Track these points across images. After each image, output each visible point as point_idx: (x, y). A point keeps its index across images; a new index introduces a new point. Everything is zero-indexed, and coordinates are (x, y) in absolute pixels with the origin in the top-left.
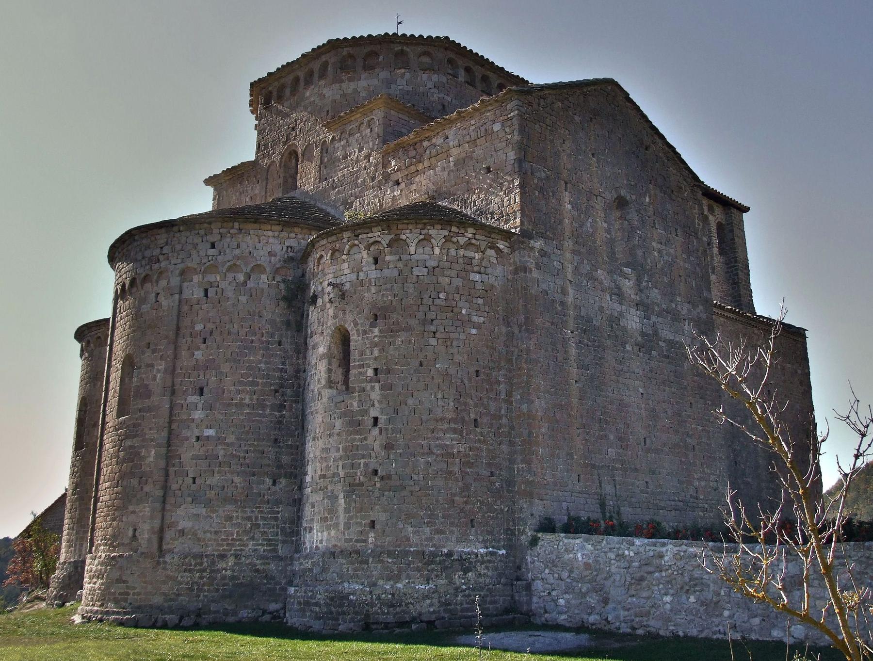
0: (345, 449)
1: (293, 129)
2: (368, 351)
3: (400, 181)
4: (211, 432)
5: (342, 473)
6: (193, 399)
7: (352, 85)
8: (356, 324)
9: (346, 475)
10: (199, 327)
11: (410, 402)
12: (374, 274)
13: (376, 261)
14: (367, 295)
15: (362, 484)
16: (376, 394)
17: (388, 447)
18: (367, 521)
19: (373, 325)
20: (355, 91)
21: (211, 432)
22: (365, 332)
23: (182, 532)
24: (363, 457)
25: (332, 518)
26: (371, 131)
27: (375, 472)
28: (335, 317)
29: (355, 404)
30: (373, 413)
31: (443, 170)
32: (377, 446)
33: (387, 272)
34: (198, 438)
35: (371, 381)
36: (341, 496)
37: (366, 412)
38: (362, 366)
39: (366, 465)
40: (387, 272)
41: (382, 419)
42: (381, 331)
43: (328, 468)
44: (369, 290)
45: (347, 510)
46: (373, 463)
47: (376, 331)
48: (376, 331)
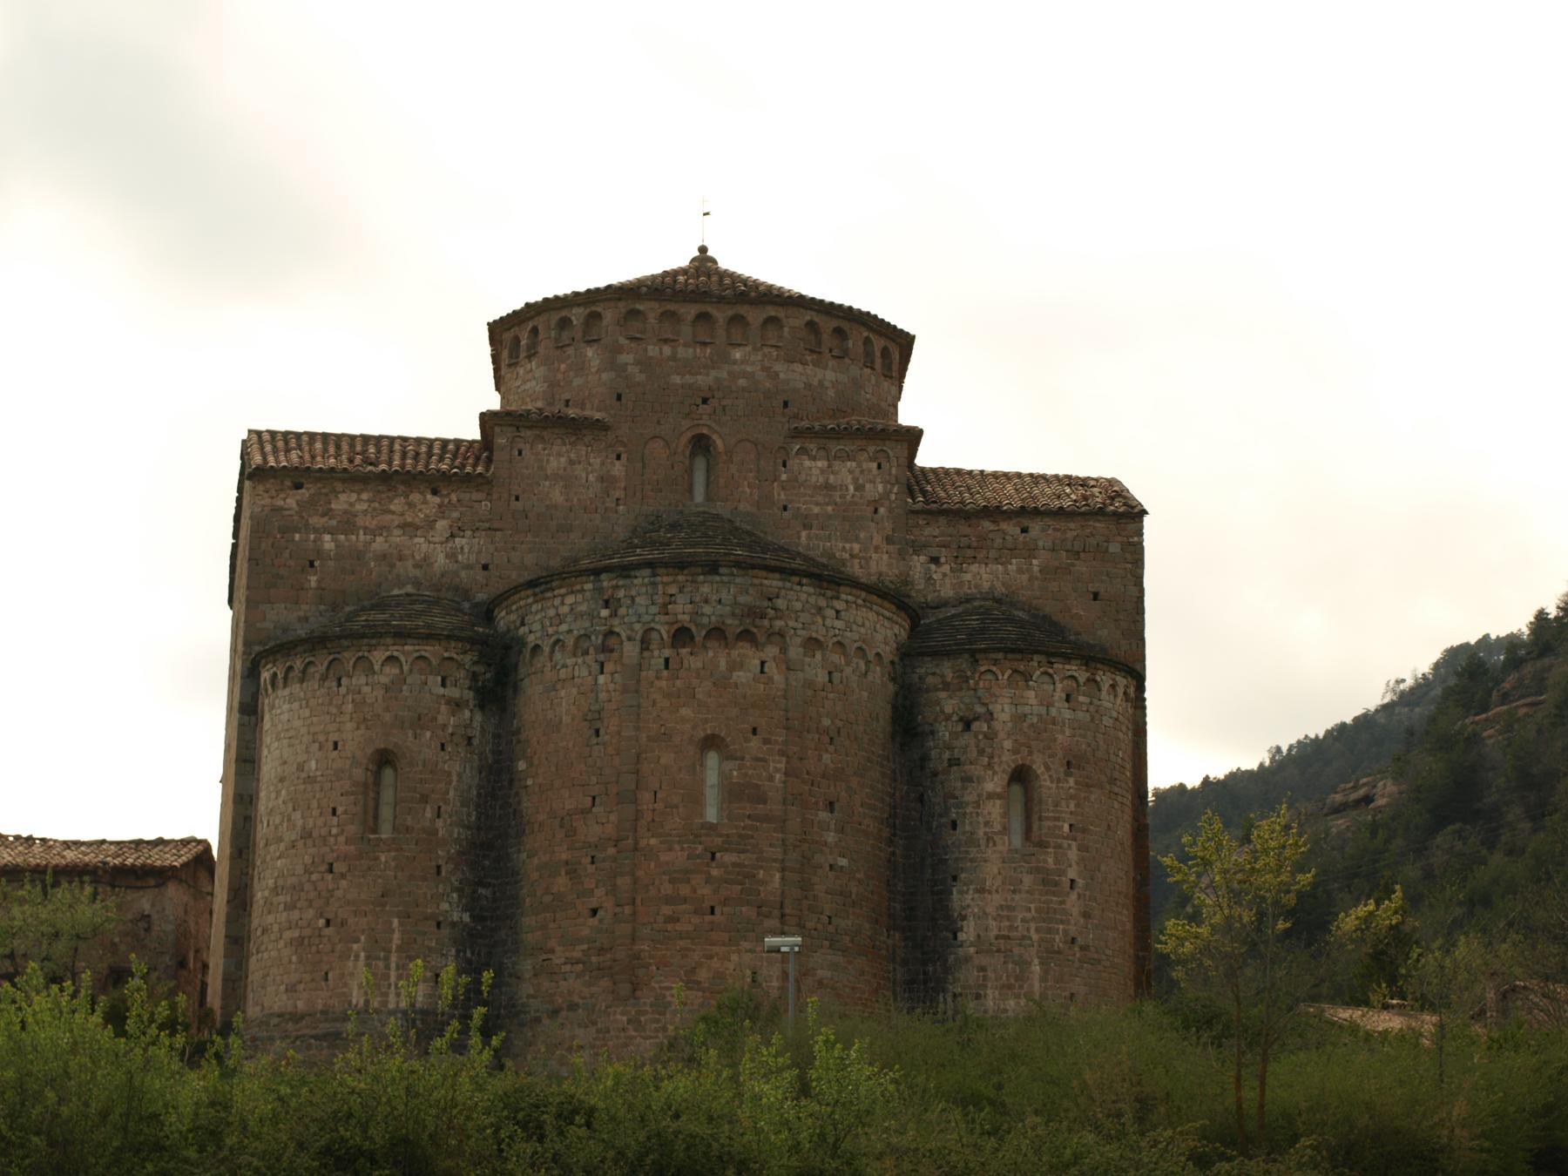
0: (1038, 910)
1: (705, 401)
2: (1063, 803)
3: (943, 560)
4: (843, 862)
5: (1035, 937)
6: (823, 815)
7: (820, 373)
8: (1048, 768)
9: (1041, 940)
10: (826, 722)
11: (1103, 868)
12: (1067, 714)
13: (1068, 699)
14: (1060, 737)
15: (1059, 952)
16: (1073, 854)
17: (1086, 915)
18: (1067, 994)
19: (1068, 774)
20: (821, 383)
21: (843, 862)
22: (1059, 781)
23: (820, 983)
24: (1062, 922)
25: (1021, 987)
26: (879, 467)
27: (1073, 940)
28: (1015, 751)
29: (1050, 860)
30: (1072, 873)
31: (1020, 571)
32: (1075, 911)
33: (1080, 715)
34: (831, 866)
35: (1066, 838)
36: (1036, 961)
37: (1062, 873)
38: (1057, 819)
39: (1065, 931)
40: (1080, 715)
41: (1080, 882)
42: (1076, 783)
43: (1011, 928)
44: (1063, 732)
45: (1043, 979)
46: (1073, 931)
47: (1071, 781)
48: (1071, 781)
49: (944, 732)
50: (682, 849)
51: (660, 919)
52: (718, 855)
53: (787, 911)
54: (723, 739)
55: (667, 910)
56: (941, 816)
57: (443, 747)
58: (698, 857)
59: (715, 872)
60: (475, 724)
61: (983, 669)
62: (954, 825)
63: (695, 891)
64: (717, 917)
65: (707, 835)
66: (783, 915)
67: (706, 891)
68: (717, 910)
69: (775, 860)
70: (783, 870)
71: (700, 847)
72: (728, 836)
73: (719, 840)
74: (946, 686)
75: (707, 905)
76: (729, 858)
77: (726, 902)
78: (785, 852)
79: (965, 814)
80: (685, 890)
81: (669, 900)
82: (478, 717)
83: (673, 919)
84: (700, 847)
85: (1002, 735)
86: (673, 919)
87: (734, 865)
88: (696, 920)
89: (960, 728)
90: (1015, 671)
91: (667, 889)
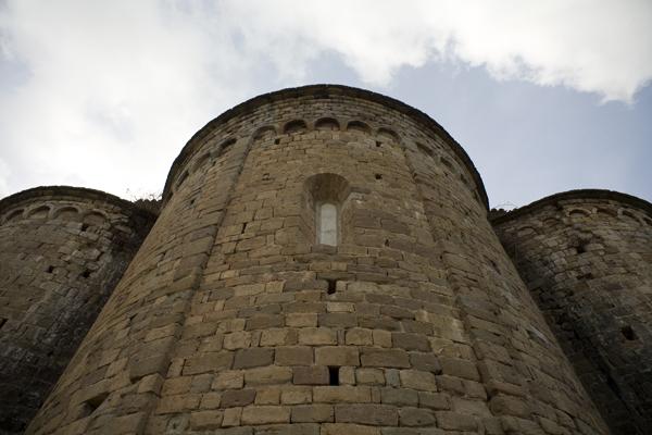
49: (559, 259)
50: (277, 279)
51: (213, 399)
52: (341, 284)
53: (498, 383)
54: (341, 178)
55: (230, 379)
56: (602, 327)
57: (50, 270)
58: (305, 286)
59: (335, 308)
60: (101, 262)
61: (571, 209)
62: (629, 334)
63: (294, 338)
64: (344, 391)
65: (319, 259)
66: (491, 394)
67: (321, 336)
68: (345, 375)
69: (443, 300)
70: (462, 316)
71: (308, 275)
72: (356, 260)
73: (343, 266)
74: (539, 231)
75: (322, 362)
76: (357, 287)
77: (361, 360)
78: (456, 289)
79: (636, 319)
80: (273, 337)
81: (236, 359)
82: (107, 258)
83: (242, 397)
84: (308, 275)
85: (623, 250)
86: (242, 397)
87: (373, 298)
88: (293, 395)
89: (574, 252)
90: (599, 210)
91: (239, 339)
